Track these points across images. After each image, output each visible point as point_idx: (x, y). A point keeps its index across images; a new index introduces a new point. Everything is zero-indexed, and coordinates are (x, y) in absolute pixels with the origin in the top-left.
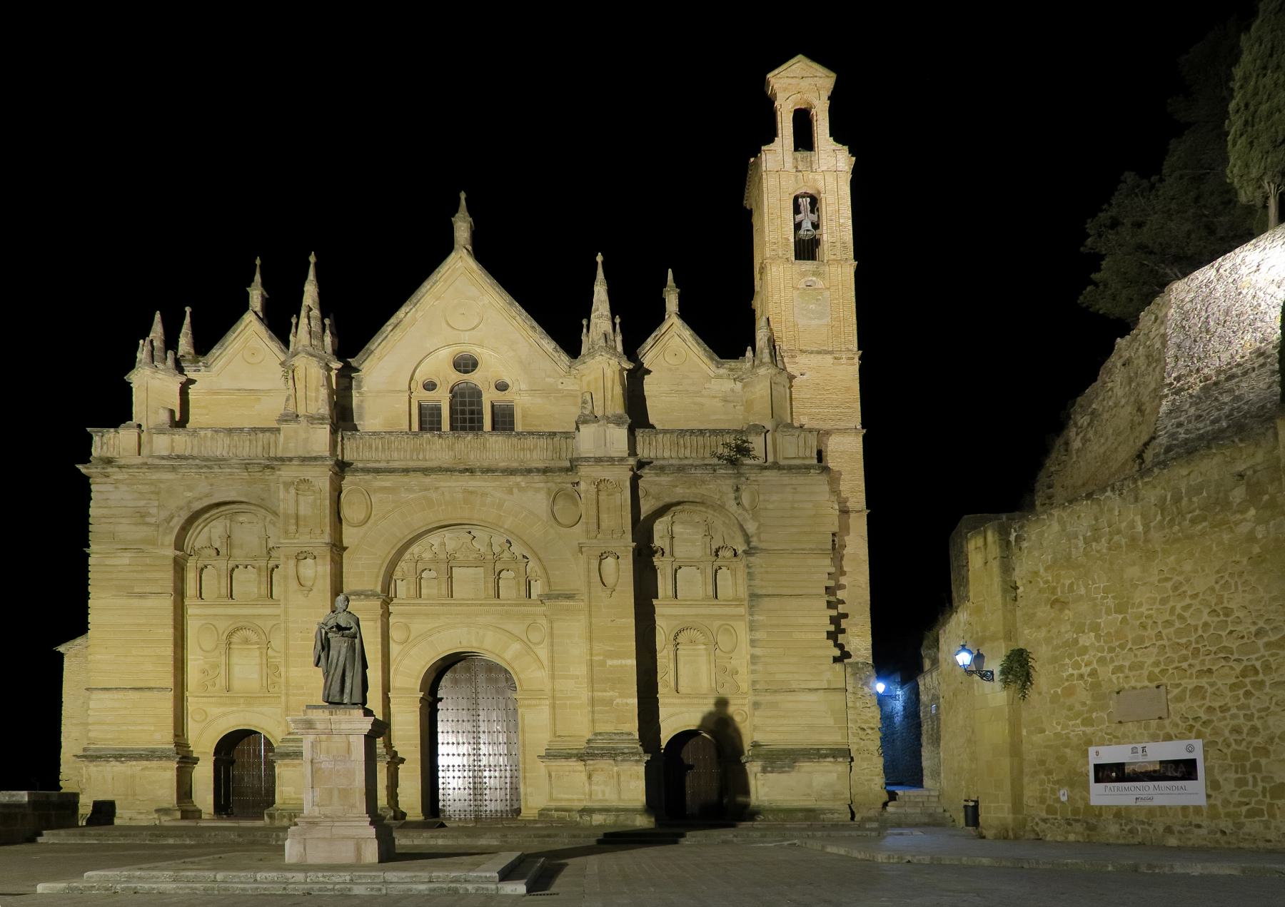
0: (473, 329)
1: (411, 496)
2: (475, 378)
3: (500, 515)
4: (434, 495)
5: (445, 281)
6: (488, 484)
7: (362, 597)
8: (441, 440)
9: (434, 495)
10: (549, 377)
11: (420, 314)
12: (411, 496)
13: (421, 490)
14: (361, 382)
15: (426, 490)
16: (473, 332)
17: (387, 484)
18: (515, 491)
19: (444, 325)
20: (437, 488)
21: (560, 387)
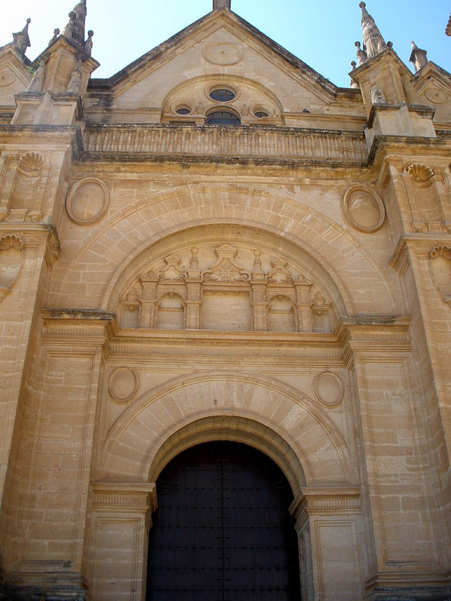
0: (234, 64)
1: (162, 191)
2: (236, 104)
3: (279, 217)
4: (191, 191)
5: (205, 31)
6: (262, 179)
7: (79, 316)
8: (203, 135)
9: (191, 191)
10: (314, 104)
11: (179, 50)
12: (162, 191)
13: (175, 185)
14: (111, 101)
15: (182, 184)
16: (234, 67)
17: (134, 176)
18: (297, 189)
19: (202, 60)
20: (196, 183)
21: (326, 112)
